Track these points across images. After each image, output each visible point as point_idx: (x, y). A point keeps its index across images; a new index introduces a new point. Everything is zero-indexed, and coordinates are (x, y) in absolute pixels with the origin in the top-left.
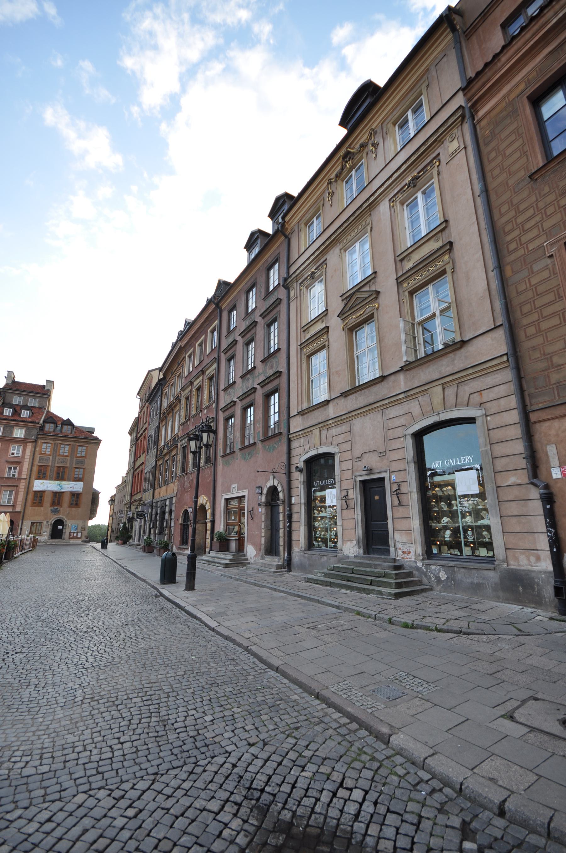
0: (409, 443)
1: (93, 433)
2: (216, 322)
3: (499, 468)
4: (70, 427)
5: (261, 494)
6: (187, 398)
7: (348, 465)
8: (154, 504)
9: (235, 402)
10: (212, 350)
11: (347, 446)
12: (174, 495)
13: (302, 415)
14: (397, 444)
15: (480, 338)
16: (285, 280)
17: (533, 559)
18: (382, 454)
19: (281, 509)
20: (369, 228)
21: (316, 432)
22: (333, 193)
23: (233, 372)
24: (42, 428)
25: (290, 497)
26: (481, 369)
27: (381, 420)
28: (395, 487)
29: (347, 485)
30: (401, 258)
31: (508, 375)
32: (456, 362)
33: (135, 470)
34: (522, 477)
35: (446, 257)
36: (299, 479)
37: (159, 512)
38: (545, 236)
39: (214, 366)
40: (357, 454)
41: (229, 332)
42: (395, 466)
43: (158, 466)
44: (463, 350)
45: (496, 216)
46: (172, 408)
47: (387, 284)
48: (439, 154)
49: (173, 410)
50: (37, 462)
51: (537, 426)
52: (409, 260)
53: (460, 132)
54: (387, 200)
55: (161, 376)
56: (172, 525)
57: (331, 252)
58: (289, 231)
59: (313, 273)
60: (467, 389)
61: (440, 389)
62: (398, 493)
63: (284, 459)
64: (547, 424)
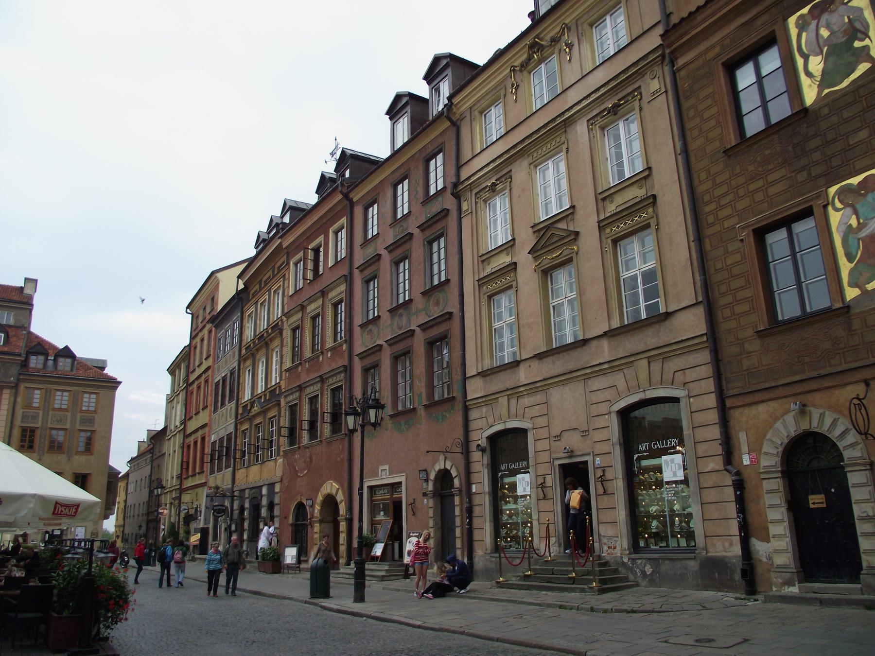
0: (614, 422)
1: (103, 368)
2: (344, 220)
3: (700, 454)
4: (69, 361)
5: (427, 480)
6: (294, 330)
7: (544, 445)
8: (236, 493)
9: (381, 346)
10: (337, 263)
11: (542, 422)
12: (278, 479)
13: (484, 376)
14: (600, 422)
15: (683, 312)
16: (455, 185)
17: (727, 545)
18: (585, 433)
19: (457, 500)
20: (564, 147)
21: (503, 400)
23: (375, 300)
24: (25, 364)
25: (469, 484)
26: (684, 347)
27: (583, 392)
28: (599, 473)
29: (543, 469)
30: (604, 197)
31: (705, 356)
32: (661, 334)
34: (716, 464)
35: (650, 210)
37: (247, 505)
39: (343, 287)
40: (556, 431)
41: (366, 242)
42: (600, 448)
44: (667, 324)
46: (263, 342)
47: (587, 224)
49: (267, 344)
50: (18, 422)
51: (732, 411)
52: (612, 202)
55: (241, 286)
57: (517, 163)
58: (457, 116)
59: (494, 185)
61: (645, 363)
62: (602, 480)
63: (459, 433)
64: (740, 410)
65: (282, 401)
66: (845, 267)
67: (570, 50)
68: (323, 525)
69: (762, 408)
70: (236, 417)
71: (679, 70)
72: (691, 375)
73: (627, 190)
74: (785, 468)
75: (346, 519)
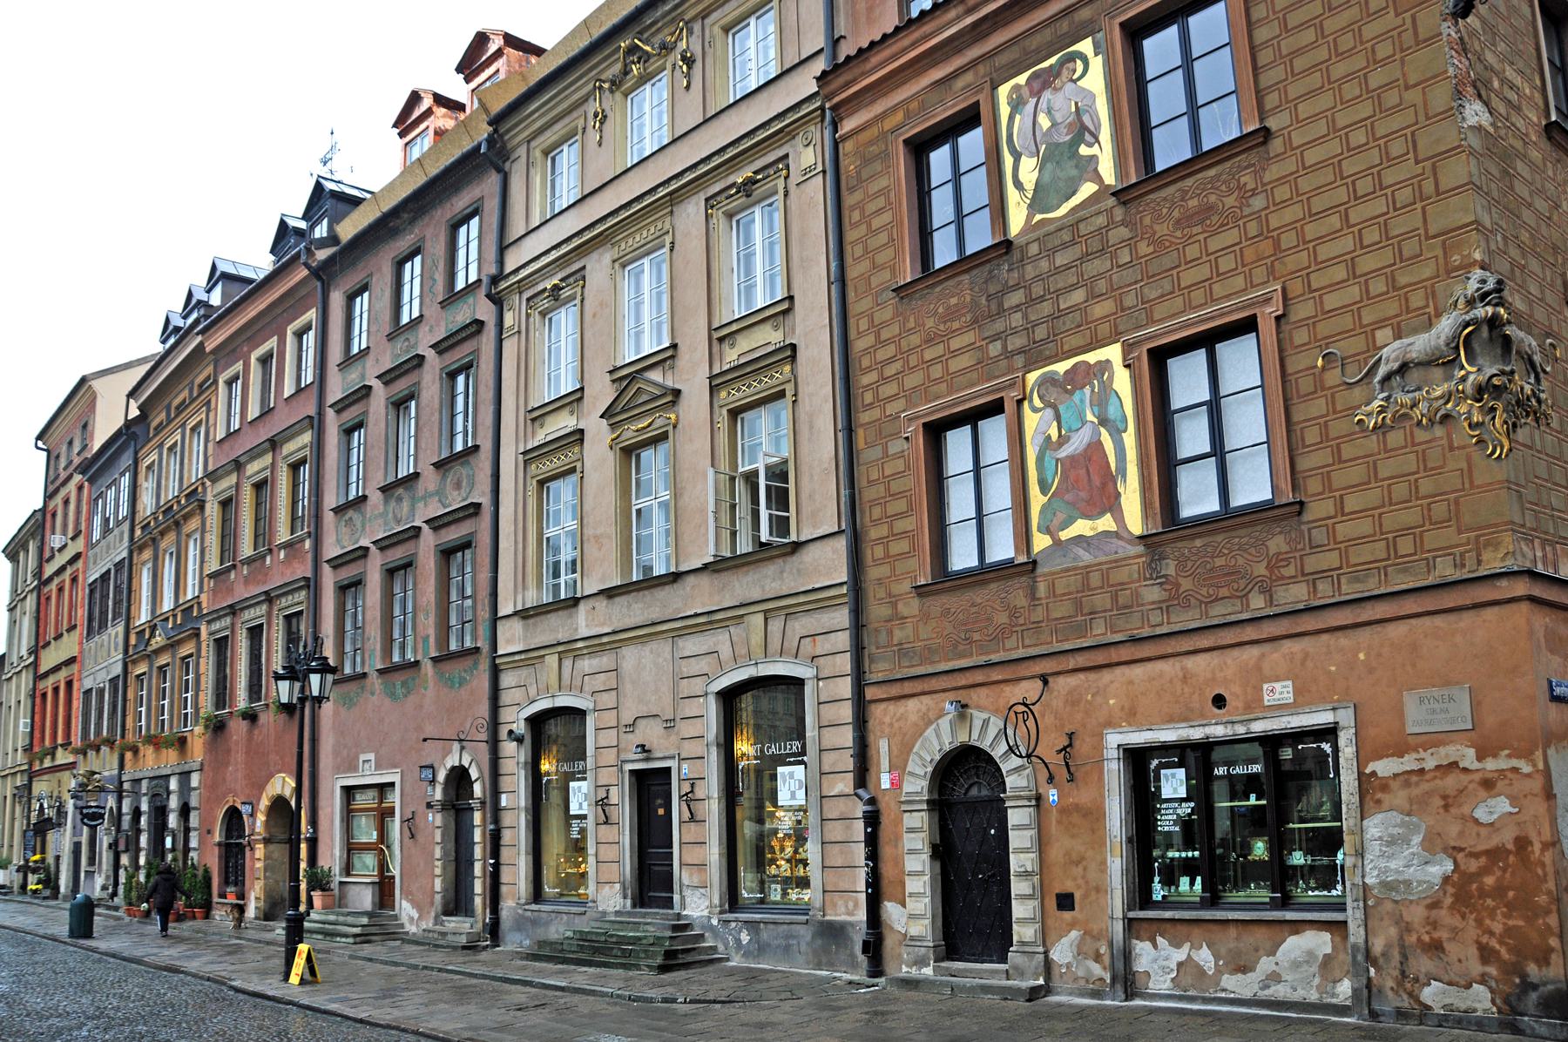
0: (712, 709)
2: (312, 315)
3: (826, 769)
5: (433, 781)
6: (226, 504)
7: (609, 738)
8: (126, 786)
9: (367, 549)
10: (299, 391)
11: (608, 700)
12: (196, 766)
13: (524, 618)
14: (691, 708)
15: (818, 544)
16: (495, 280)
19: (477, 817)
20: (668, 239)
21: (552, 660)
22: (605, 117)
23: (358, 467)
25: (496, 792)
26: (815, 600)
27: (669, 657)
28: (686, 788)
29: (607, 776)
30: (721, 336)
31: (842, 617)
33: (39, 678)
35: (787, 368)
36: (514, 756)
37: (144, 807)
38: (903, 401)
39: (307, 437)
40: (627, 718)
41: (349, 360)
42: (690, 749)
43: (131, 680)
44: (795, 560)
45: (852, 334)
46: (173, 519)
47: (692, 378)
48: (787, 156)
49: (177, 524)
51: (873, 706)
52: (732, 346)
53: (819, 135)
54: (702, 196)
55: (134, 412)
56: (193, 843)
57: (595, 255)
59: (556, 288)
60: (801, 625)
61: (760, 618)
62: (689, 799)
63: (484, 709)
64: (883, 706)
65: (204, 629)
66: (1037, 500)
67: (689, 68)
68: (272, 847)
69: (912, 704)
70: (126, 651)
71: (845, 138)
72: (823, 645)
73: (756, 328)
74: (936, 796)
75: (307, 839)
